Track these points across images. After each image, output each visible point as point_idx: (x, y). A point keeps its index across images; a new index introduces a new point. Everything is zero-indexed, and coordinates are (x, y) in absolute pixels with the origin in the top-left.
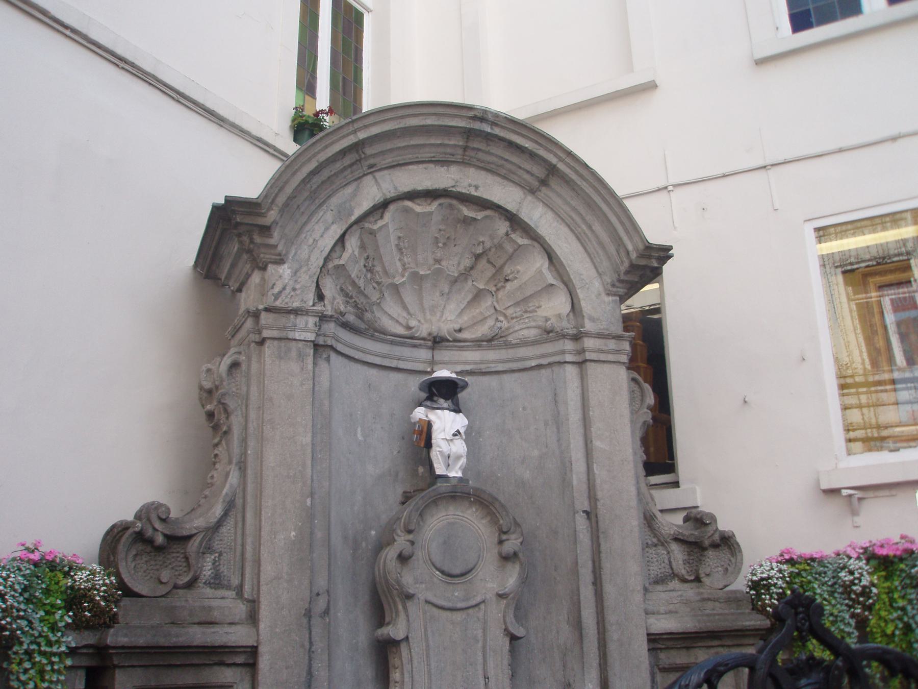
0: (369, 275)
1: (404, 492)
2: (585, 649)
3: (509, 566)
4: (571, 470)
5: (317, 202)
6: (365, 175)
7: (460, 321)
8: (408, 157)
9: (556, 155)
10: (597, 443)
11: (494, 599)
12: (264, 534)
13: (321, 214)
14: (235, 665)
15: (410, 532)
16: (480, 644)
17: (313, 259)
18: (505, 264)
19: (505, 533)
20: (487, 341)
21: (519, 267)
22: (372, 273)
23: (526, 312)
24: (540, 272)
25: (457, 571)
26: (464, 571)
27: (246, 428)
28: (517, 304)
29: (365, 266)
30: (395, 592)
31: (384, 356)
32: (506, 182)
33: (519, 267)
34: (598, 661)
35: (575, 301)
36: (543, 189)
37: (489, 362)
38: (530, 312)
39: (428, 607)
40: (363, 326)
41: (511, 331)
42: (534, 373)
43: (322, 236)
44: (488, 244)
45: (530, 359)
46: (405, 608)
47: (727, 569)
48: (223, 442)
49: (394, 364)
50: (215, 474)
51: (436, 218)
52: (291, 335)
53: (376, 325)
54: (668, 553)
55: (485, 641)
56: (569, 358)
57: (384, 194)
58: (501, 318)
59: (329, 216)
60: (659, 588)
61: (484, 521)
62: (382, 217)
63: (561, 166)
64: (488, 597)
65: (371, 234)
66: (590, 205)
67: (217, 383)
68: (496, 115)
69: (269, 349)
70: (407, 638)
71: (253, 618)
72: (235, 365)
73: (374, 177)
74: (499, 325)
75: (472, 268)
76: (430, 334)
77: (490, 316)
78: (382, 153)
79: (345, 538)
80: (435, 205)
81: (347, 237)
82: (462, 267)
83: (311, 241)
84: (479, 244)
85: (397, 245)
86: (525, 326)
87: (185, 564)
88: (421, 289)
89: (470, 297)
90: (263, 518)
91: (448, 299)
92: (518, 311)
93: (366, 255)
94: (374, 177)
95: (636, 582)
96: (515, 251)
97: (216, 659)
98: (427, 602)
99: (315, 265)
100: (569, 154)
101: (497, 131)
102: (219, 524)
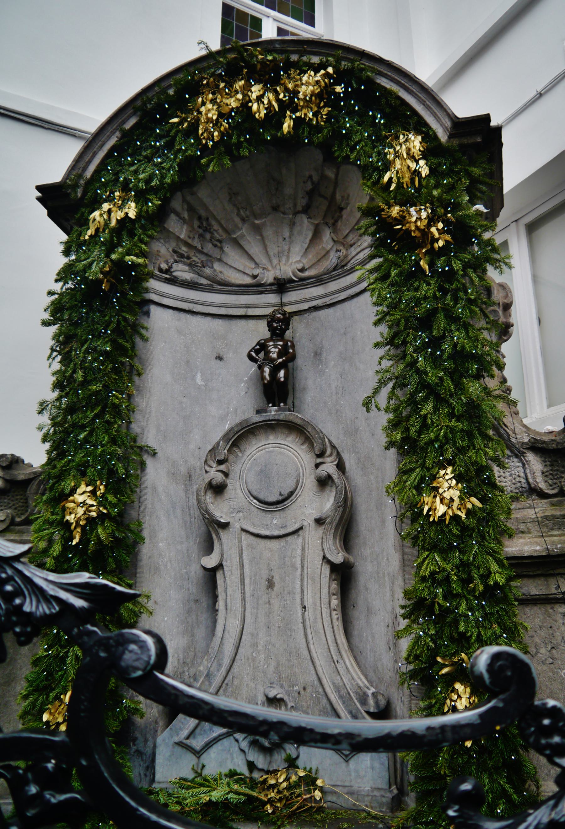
0: (208, 236)
7: (305, 261)
11: (313, 524)
15: (220, 462)
18: (334, 193)
22: (210, 232)
37: (333, 293)
39: (243, 535)
40: (204, 281)
41: (350, 257)
46: (218, 535)
49: (241, 312)
53: (218, 279)
55: (303, 567)
58: (341, 248)
64: (305, 523)
76: (275, 279)
77: (331, 249)
79: (174, 474)
86: (359, 250)
89: (310, 235)
91: (291, 242)
96: (337, 175)
98: (243, 530)
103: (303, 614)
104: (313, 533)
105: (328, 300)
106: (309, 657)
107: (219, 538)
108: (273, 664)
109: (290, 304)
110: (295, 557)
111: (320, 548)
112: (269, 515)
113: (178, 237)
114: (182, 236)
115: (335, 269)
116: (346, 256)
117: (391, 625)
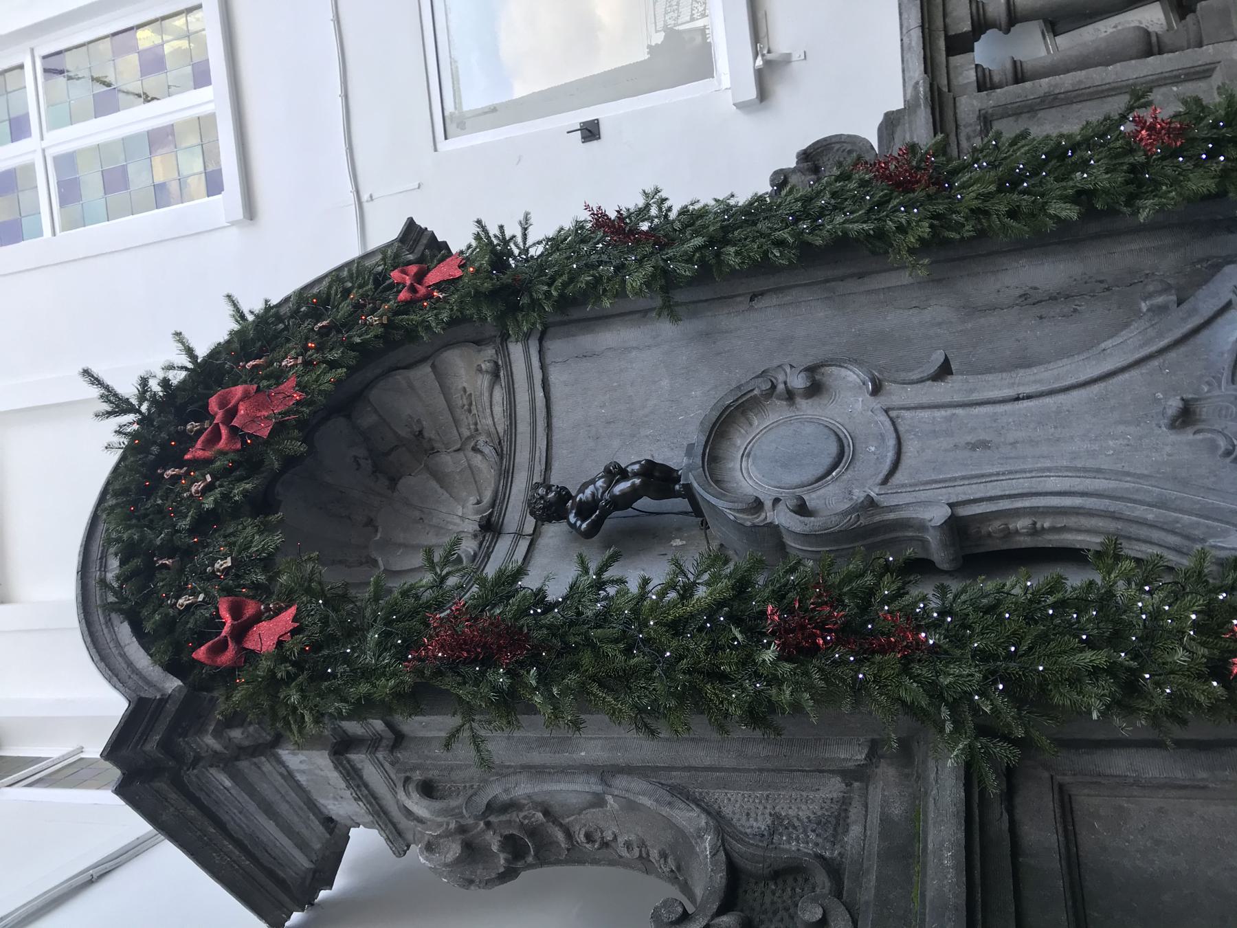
3: (828, 381)
16: (959, 411)
18: (395, 433)
19: (774, 387)
20: (502, 459)
23: (470, 411)
25: (833, 449)
30: (862, 521)
37: (532, 459)
38: (471, 404)
41: (492, 429)
42: (556, 392)
45: (533, 400)
46: (891, 509)
50: (621, 840)
61: (756, 423)
67: (453, 826)
70: (951, 505)
72: (428, 790)
74: (481, 445)
76: (475, 536)
84: (359, 464)
86: (488, 411)
87: (790, 881)
88: (405, 546)
89: (434, 484)
98: (885, 481)
102: (715, 815)
104: (894, 398)
106: (1102, 385)
108: (1121, 428)
111: (919, 386)
112: (860, 456)
115: (500, 455)
116: (489, 434)
117: (1036, 310)
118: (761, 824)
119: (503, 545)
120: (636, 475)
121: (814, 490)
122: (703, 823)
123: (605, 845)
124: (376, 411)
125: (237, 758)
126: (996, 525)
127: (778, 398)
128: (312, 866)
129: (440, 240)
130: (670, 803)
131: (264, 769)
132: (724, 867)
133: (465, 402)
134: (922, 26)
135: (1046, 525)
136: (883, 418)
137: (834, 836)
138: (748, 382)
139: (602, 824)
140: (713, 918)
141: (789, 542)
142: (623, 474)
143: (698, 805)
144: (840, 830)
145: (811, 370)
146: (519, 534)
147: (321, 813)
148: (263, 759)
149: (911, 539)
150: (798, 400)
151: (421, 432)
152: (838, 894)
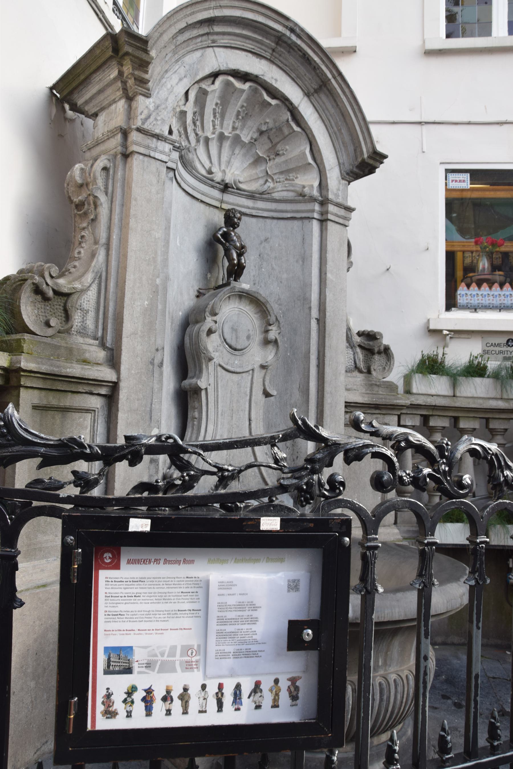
1: (199, 289)
2: (310, 407)
4: (311, 291)
5: (177, 57)
6: (208, 47)
8: (238, 43)
9: (331, 72)
10: (329, 275)
12: (126, 299)
13: (177, 67)
14: (99, 395)
16: (248, 398)
17: (170, 101)
18: (278, 143)
19: (270, 325)
21: (287, 147)
23: (286, 179)
24: (304, 154)
26: (242, 347)
27: (110, 219)
28: (281, 173)
29: (193, 119)
31: (194, 189)
32: (293, 83)
33: (287, 147)
34: (316, 416)
35: (322, 178)
36: (316, 95)
38: (290, 180)
39: (219, 368)
41: (275, 190)
43: (177, 84)
44: (271, 125)
45: (286, 211)
47: (385, 368)
48: (90, 228)
51: (244, 96)
52: (152, 154)
54: (354, 354)
56: (316, 215)
57: (219, 66)
58: (270, 180)
59: (182, 71)
60: (349, 374)
62: (213, 83)
63: (333, 81)
65: (204, 94)
66: (344, 115)
67: (89, 180)
68: (302, 30)
69: (136, 161)
71: (114, 361)
72: (105, 169)
73: (214, 51)
75: (255, 140)
76: (223, 181)
77: (262, 177)
78: (224, 34)
79: (169, 313)
80: (247, 86)
81: (190, 91)
82: (249, 138)
83: (169, 86)
85: (214, 110)
86: (285, 189)
89: (251, 160)
90: (126, 288)
92: (282, 177)
93: (195, 110)
94: (214, 51)
95: (342, 369)
96: (290, 134)
97: (87, 389)
99: (171, 105)
100: (340, 74)
101: (299, 42)
102: (88, 288)
103: (250, 424)
105: (254, 212)
107: (207, 368)
109: (227, 203)
110: (247, 388)
111: (262, 384)
112: (233, 357)
113: (186, 122)
114: (187, 123)
115: (262, 193)
118: (85, 306)
119: (216, 193)
120: (239, 260)
121: (220, 337)
122: (85, 284)
123: (80, 243)
124: (290, 134)
125: (122, 82)
126: (196, 404)
127: (266, 326)
128: (78, 105)
129: (377, 170)
130: (93, 271)
131: (117, 92)
132: (69, 292)
133: (291, 178)
134: (435, 406)
135: (195, 423)
136: (250, 368)
137: (79, 332)
138: (274, 314)
139: (88, 243)
140: (51, 287)
141: (198, 326)
142: (240, 255)
143: (92, 283)
144: (81, 334)
145: (276, 342)
146: (222, 201)
147: (100, 112)
148: (121, 93)
149: (195, 373)
150: (264, 335)
151: (278, 155)
152: (59, 332)
